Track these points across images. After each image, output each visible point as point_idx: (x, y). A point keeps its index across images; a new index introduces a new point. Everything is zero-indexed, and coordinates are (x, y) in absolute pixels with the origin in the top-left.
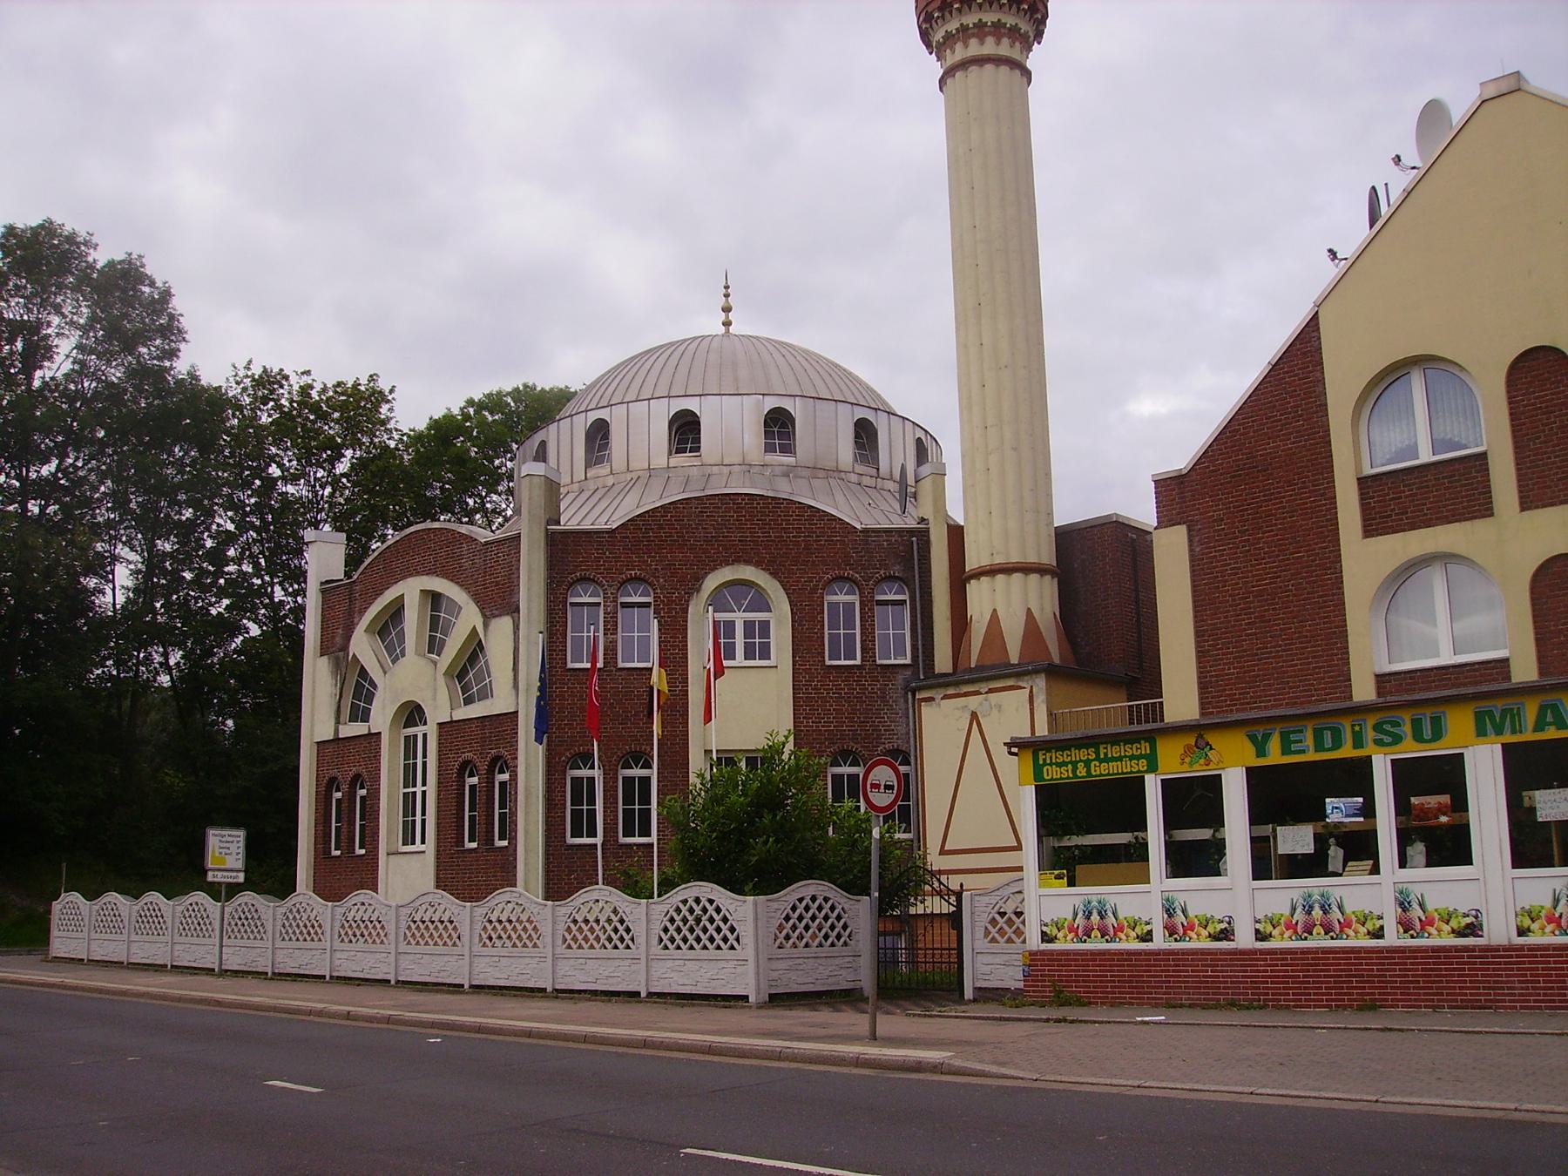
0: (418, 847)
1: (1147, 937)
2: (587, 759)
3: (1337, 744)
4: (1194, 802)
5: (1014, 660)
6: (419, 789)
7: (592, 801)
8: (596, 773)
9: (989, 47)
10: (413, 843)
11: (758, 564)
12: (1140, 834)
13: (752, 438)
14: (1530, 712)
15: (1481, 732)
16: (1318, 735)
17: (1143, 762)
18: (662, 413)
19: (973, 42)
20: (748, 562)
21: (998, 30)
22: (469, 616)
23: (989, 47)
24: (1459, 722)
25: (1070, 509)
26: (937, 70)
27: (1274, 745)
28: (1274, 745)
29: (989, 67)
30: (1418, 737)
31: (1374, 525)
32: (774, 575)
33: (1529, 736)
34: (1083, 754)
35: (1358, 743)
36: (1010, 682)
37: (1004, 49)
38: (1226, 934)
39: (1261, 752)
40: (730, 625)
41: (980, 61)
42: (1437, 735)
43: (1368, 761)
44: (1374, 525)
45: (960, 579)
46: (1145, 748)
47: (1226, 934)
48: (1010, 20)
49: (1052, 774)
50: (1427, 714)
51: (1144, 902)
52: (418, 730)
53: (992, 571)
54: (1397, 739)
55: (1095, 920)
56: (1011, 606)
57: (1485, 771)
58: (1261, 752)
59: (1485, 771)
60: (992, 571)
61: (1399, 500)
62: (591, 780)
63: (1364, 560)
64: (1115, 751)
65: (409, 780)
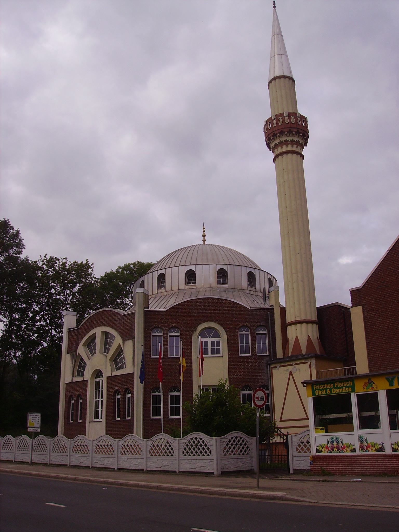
0: (100, 420)
1: (354, 450)
2: (158, 389)
4: (368, 402)
5: (304, 353)
6: (100, 399)
7: (159, 404)
8: (161, 394)
9: (289, 148)
10: (98, 418)
12: (350, 414)
13: (213, 279)
18: (182, 271)
20: (212, 321)
21: (292, 143)
22: (118, 340)
23: (289, 148)
27: (396, 382)
28: (396, 382)
29: (290, 155)
32: (221, 325)
34: (329, 386)
37: (295, 149)
38: (382, 449)
39: (391, 384)
40: (206, 343)
41: (287, 153)
46: (351, 384)
48: (296, 139)
49: (319, 393)
51: (352, 438)
52: (100, 379)
53: (295, 323)
55: (335, 445)
60: (295, 323)
62: (159, 396)
64: (340, 385)
65: (97, 396)
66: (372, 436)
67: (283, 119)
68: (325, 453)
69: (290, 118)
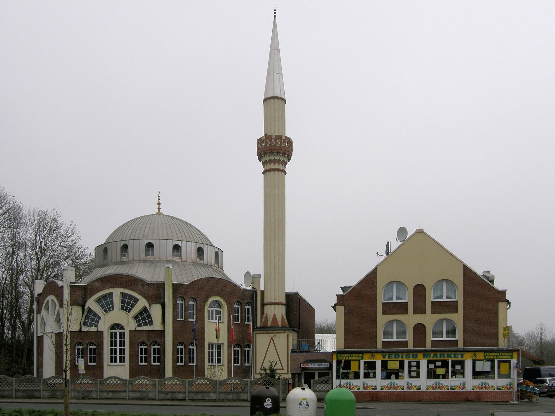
1: (359, 389)
2: (192, 343)
3: (398, 357)
4: (371, 366)
5: (280, 326)
7: (193, 354)
8: (194, 347)
9: (277, 166)
11: (220, 296)
12: (366, 371)
14: (432, 355)
15: (424, 357)
16: (395, 355)
17: (360, 358)
19: (272, 164)
20: (218, 296)
23: (277, 166)
24: (420, 355)
25: (289, 289)
26: (263, 170)
27: (387, 356)
28: (387, 356)
30: (413, 357)
31: (384, 313)
32: (224, 299)
33: (431, 359)
34: (348, 355)
35: (402, 357)
36: (283, 331)
37: (280, 167)
39: (384, 358)
40: (212, 311)
42: (416, 357)
43: (403, 361)
44: (384, 313)
45: (263, 305)
46: (361, 355)
48: (282, 159)
50: (415, 354)
54: (409, 357)
56: (278, 313)
57: (424, 363)
58: (384, 358)
59: (424, 363)
61: (389, 308)
62: (193, 349)
63: (382, 320)
64: (355, 355)
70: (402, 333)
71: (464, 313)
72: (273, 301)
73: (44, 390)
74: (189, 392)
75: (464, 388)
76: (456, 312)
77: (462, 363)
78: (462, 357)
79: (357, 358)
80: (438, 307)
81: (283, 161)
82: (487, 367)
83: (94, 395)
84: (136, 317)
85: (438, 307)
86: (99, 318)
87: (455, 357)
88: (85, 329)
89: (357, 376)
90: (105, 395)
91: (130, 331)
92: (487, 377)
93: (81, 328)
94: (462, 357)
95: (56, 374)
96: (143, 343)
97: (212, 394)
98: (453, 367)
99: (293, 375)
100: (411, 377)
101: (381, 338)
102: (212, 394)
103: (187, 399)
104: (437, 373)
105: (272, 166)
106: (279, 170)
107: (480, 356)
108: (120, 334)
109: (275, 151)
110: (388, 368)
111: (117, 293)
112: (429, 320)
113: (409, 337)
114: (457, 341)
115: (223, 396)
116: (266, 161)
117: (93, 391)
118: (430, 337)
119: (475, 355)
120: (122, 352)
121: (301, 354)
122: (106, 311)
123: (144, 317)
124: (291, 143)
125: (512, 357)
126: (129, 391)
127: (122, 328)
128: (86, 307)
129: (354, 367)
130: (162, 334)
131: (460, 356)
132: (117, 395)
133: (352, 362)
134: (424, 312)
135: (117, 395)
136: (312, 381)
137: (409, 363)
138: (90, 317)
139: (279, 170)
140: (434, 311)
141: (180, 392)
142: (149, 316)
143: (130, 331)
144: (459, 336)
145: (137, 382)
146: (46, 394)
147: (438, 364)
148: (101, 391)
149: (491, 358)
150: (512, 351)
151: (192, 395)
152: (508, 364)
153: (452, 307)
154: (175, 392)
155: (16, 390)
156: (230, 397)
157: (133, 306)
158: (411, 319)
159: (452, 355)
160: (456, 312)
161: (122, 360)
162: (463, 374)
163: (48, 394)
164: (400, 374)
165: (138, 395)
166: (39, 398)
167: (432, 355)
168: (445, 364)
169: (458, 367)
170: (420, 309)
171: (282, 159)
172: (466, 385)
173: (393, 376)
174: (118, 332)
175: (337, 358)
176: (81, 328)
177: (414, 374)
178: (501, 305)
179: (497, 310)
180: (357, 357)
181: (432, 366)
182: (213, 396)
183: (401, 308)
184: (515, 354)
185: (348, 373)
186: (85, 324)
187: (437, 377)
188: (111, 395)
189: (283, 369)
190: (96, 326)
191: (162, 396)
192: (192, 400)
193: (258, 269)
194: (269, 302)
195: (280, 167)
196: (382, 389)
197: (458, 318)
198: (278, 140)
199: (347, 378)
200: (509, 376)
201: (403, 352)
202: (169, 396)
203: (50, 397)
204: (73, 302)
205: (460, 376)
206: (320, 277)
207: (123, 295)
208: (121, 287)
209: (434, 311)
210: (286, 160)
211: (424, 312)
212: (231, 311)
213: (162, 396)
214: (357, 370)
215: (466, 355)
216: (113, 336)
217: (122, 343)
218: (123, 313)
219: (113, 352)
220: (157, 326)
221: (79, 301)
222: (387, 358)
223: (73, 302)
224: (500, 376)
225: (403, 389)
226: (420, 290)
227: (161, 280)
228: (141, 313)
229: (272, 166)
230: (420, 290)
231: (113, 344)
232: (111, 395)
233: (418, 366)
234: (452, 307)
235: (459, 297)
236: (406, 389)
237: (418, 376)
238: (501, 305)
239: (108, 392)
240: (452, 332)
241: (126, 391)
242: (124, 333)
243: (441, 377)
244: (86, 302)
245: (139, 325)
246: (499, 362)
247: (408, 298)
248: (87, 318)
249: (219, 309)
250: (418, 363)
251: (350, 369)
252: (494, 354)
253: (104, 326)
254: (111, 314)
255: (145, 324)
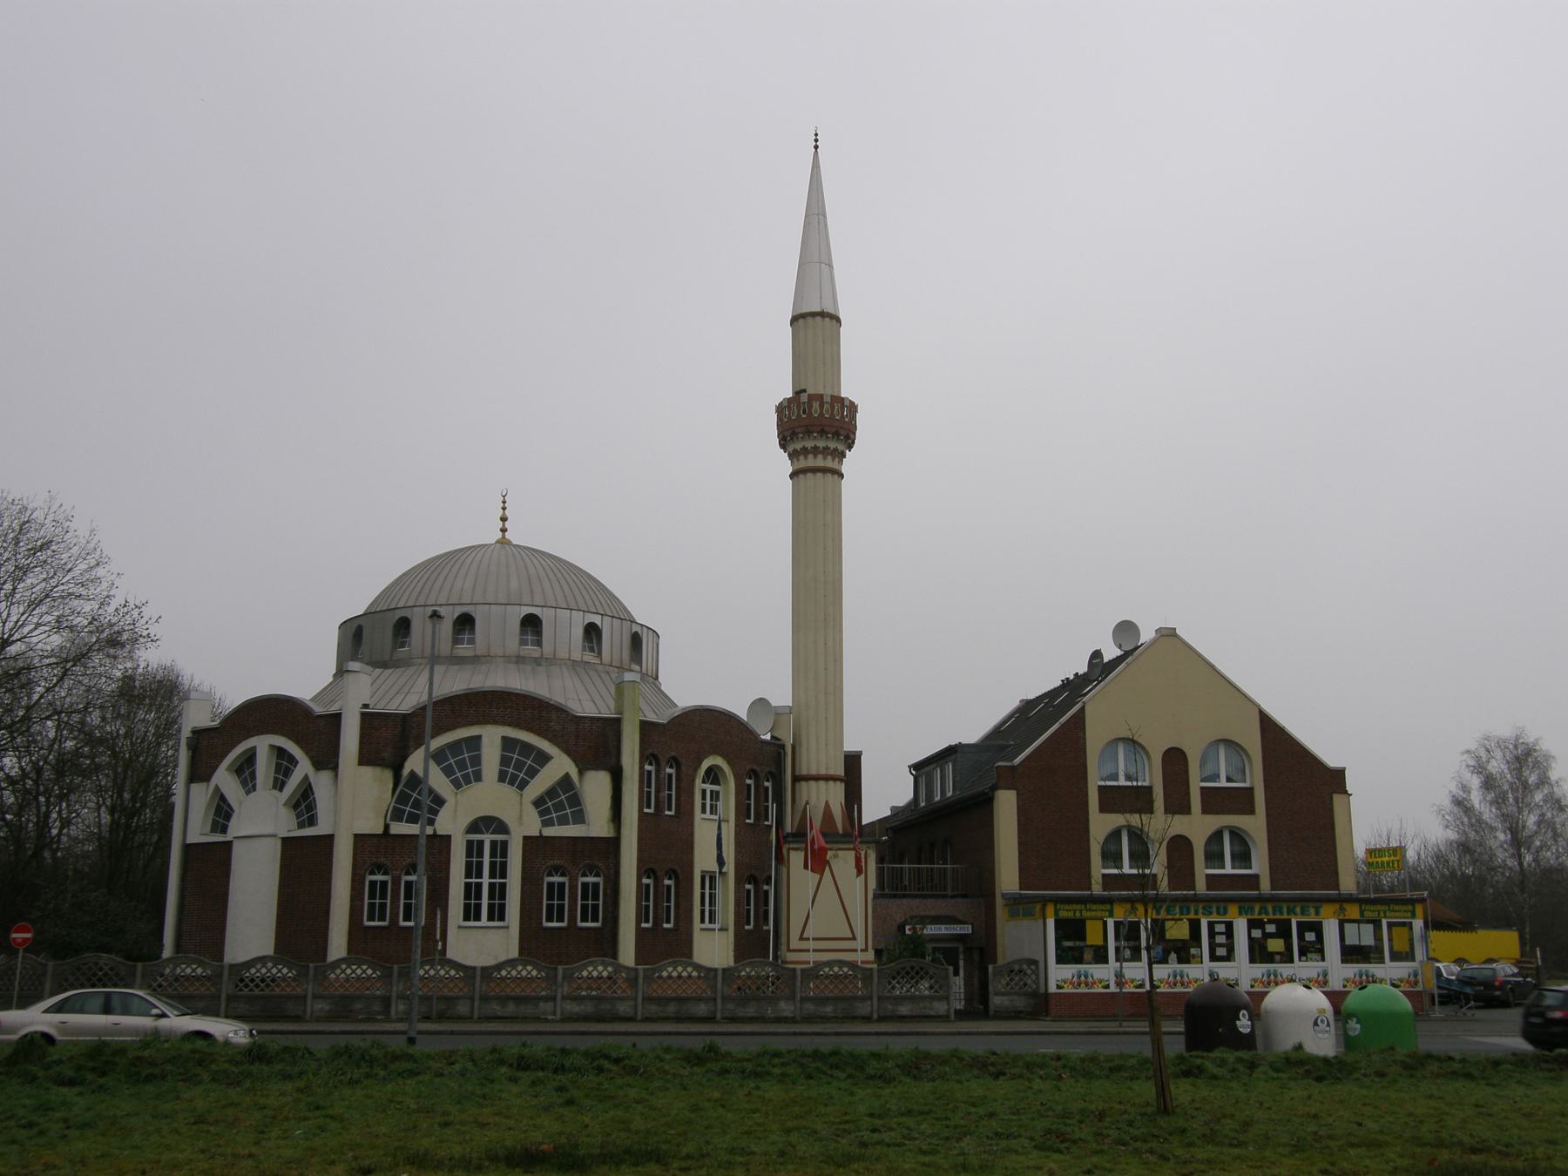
9: (820, 462)
14: (1257, 909)
21: (826, 452)
23: (820, 462)
24: (1233, 909)
25: (849, 746)
29: (819, 475)
31: (1104, 808)
37: (829, 463)
41: (814, 470)
42: (1225, 913)
44: (1104, 808)
47: (1141, 986)
48: (832, 445)
49: (1064, 914)
50: (1222, 905)
51: (1103, 973)
57: (1240, 926)
59: (1240, 926)
61: (1113, 799)
63: (1101, 824)
66: (1225, 971)
67: (821, 406)
68: (1068, 989)
69: (833, 407)
70: (1141, 856)
71: (1268, 816)
72: (823, 772)
73: (315, 997)
74: (723, 998)
75: (1416, 983)
76: (1252, 811)
77: (1317, 928)
78: (1317, 913)
79: (1099, 914)
80: (1216, 801)
81: (836, 450)
82: (1368, 939)
83: (462, 1008)
84: (538, 803)
85: (1216, 801)
86: (440, 801)
87: (1303, 914)
88: (399, 828)
89: (1100, 956)
90: (496, 1008)
91: (525, 838)
92: (1367, 960)
93: (387, 827)
94: (1317, 913)
95: (350, 951)
96: (556, 870)
97: (782, 1004)
98: (1301, 937)
99: (878, 953)
100: (1214, 958)
101: (1098, 869)
102: (782, 1004)
103: (719, 1016)
104: (1270, 949)
105: (811, 462)
106: (825, 470)
107: (1353, 911)
108: (494, 844)
109: (816, 428)
110: (1168, 936)
111: (492, 737)
112: (1197, 826)
113: (1158, 866)
114: (1256, 877)
115: (810, 1007)
116: (795, 451)
117: (458, 998)
118: (1202, 871)
119: (1342, 909)
120: (499, 892)
121: (898, 901)
122: (457, 784)
123: (562, 800)
124: (853, 408)
125: (1414, 916)
126: (563, 998)
127: (502, 827)
128: (406, 772)
129: (1093, 937)
130: (610, 848)
131: (1312, 911)
132: (528, 1010)
133: (1088, 923)
134: (1185, 809)
135: (528, 1010)
136: (990, 967)
137: (1211, 925)
138: (413, 799)
139: (825, 470)
140: (1206, 810)
141: (700, 999)
142: (575, 801)
143: (525, 838)
144: (1260, 864)
145: (585, 973)
146: (322, 1006)
147: (1271, 928)
148: (485, 999)
149: (1374, 915)
150: (1413, 902)
151: (730, 1006)
152: (1406, 929)
153: (1239, 801)
154: (688, 999)
155: (229, 998)
156: (829, 1009)
157: (532, 773)
158: (1160, 825)
159: (1298, 910)
160: (1251, 811)
161: (498, 913)
162: (1321, 951)
163: (327, 1007)
164: (1193, 951)
165: (588, 1008)
166: (297, 1019)
167: (1257, 909)
168: (1284, 931)
169: (1310, 936)
170: (1178, 804)
171: (832, 445)
172: (1330, 977)
173: (1173, 956)
174: (487, 839)
175: (1056, 913)
176: (387, 827)
177: (1221, 952)
178: (1337, 798)
179: (1331, 810)
180: (1098, 911)
181: (1257, 933)
182: (786, 1008)
183: (1138, 799)
184: (1419, 909)
185: (1081, 950)
186: (398, 815)
187: (1268, 958)
188: (511, 1008)
189: (854, 938)
190: (431, 822)
191: (654, 1009)
192: (733, 1019)
193: (781, 696)
194: (814, 772)
195: (829, 463)
196: (1058, 987)
197: (1255, 825)
198: (816, 405)
199: (1079, 960)
200: (1409, 956)
201: (1186, 899)
202: (671, 1009)
203: (331, 1017)
204: (367, 757)
205: (1314, 956)
206: (899, 724)
207: (508, 744)
208: (504, 724)
209: (1206, 810)
210: (841, 447)
211: (1185, 809)
212: (742, 792)
213: (654, 1009)
214: (1100, 943)
215: (1327, 909)
216: (474, 849)
217: (499, 870)
218: (507, 790)
219: (472, 891)
220: (597, 825)
221: (385, 755)
222: (1163, 915)
223: (367, 757)
224: (1395, 956)
225: (1107, 987)
226: (1175, 760)
227: (606, 710)
228: (551, 793)
229: (811, 462)
230: (1175, 760)
231: (473, 869)
232: (511, 1008)
233: (1229, 932)
234: (1239, 801)
235: (1255, 779)
236: (1113, 989)
237: (1229, 957)
238: (1337, 798)
239: (504, 1000)
240: (1243, 857)
241: (554, 999)
242: (505, 844)
243: (1278, 958)
244: (405, 758)
245: (546, 823)
246: (1390, 925)
247: (1152, 777)
248: (403, 799)
249: (715, 788)
250: (1229, 926)
251: (1083, 938)
252: (1379, 907)
253: (452, 822)
254: (475, 790)
255: (563, 821)
